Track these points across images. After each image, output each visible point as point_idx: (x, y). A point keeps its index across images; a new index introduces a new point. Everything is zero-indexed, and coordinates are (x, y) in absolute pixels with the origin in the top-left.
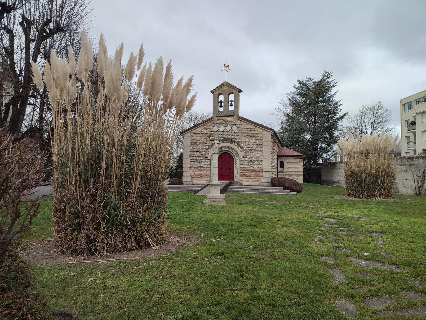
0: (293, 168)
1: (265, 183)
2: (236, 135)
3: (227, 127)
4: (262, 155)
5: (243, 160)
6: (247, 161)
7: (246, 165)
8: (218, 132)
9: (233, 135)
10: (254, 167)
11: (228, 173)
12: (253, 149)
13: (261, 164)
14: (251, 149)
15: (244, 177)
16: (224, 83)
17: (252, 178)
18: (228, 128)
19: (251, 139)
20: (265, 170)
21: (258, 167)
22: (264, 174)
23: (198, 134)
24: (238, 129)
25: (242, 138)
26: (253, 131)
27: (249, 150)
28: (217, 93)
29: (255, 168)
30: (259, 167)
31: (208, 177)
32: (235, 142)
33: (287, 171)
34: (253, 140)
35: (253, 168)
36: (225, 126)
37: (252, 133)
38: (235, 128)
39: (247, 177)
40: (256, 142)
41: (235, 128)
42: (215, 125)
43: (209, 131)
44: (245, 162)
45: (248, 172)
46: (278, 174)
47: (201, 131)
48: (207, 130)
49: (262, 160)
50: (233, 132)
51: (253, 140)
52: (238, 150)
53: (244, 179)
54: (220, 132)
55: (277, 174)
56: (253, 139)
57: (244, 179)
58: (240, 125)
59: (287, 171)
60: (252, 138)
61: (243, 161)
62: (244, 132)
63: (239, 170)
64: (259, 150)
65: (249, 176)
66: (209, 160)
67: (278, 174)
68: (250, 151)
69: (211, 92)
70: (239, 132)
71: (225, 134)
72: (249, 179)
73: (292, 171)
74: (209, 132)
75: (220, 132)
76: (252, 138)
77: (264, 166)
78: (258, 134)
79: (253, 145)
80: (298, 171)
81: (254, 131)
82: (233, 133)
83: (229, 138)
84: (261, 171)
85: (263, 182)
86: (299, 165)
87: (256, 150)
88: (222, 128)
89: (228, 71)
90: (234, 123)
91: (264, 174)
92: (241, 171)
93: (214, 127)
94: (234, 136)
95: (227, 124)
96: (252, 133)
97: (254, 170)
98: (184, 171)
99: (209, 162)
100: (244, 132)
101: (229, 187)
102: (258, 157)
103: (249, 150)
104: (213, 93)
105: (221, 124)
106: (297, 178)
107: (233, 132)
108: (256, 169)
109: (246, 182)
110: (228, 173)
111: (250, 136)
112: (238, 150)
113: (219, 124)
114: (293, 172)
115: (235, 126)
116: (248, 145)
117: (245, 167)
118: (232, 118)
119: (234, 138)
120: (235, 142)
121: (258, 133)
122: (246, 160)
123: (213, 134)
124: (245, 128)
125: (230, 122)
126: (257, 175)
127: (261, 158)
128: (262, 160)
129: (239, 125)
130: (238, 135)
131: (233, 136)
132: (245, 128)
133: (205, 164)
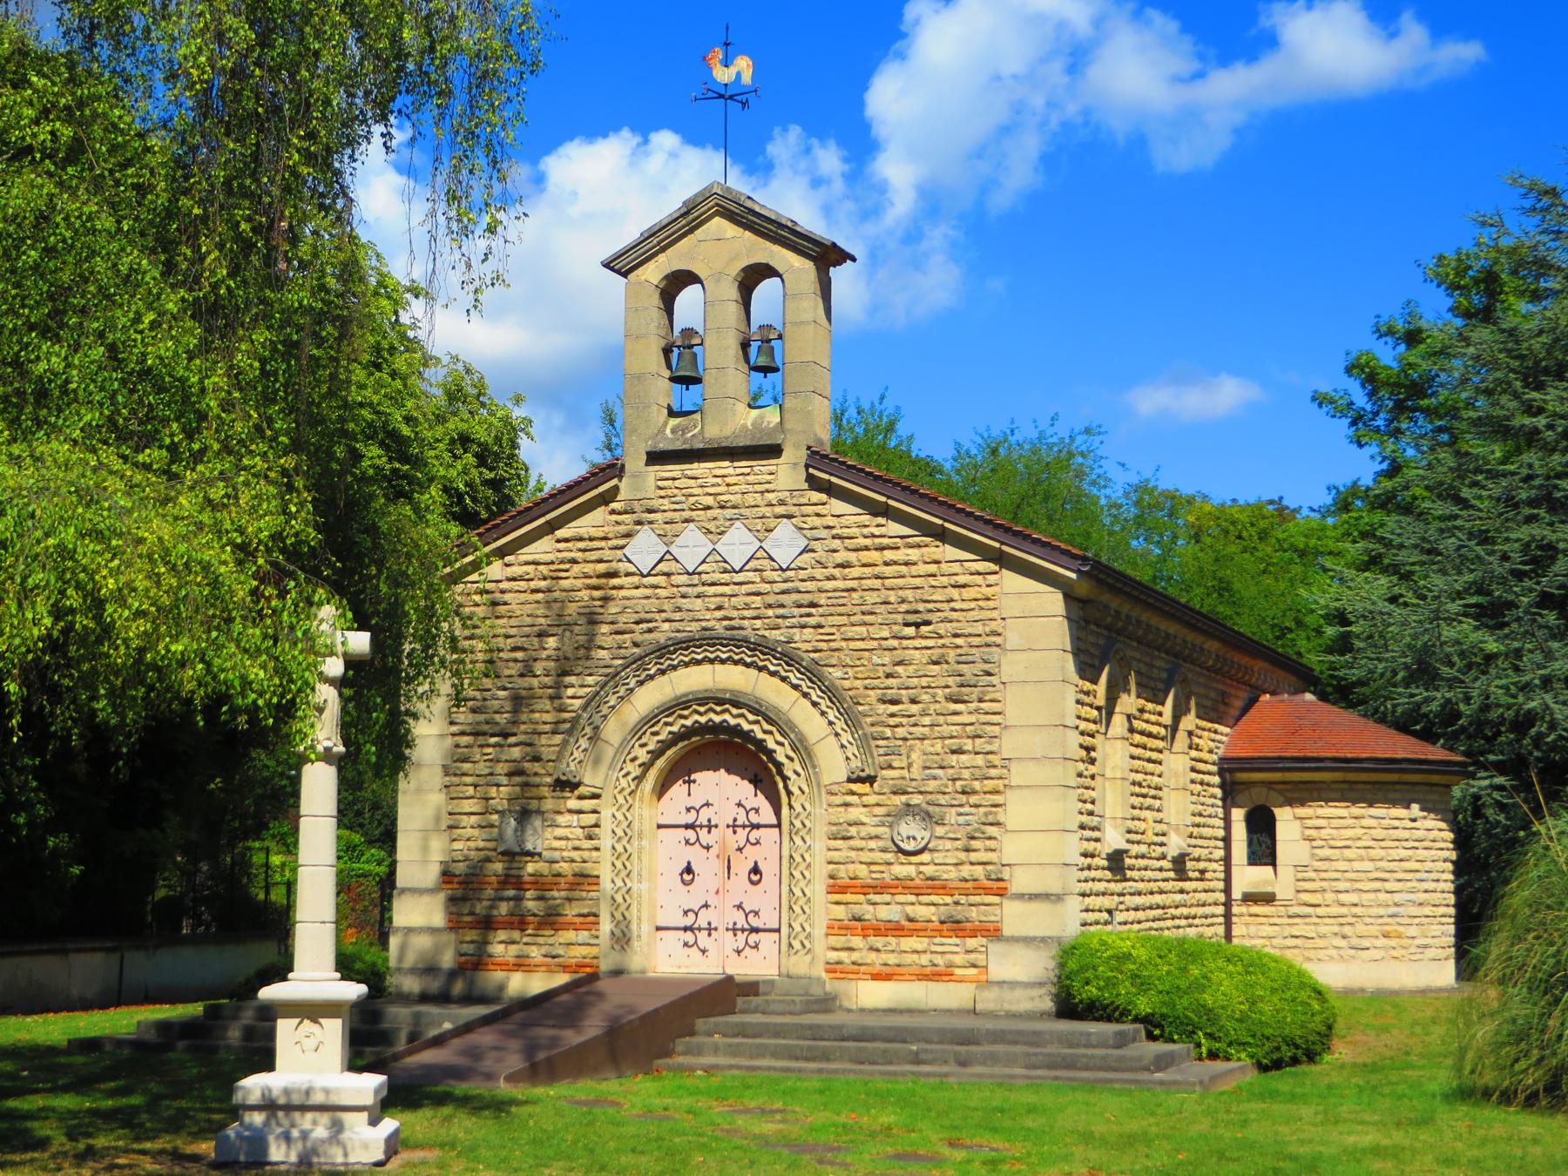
0: (1357, 865)
1: (1019, 993)
2: (795, 597)
3: (725, 538)
4: (995, 759)
5: (846, 805)
6: (878, 811)
7: (872, 844)
8: (661, 580)
9: (771, 599)
10: (938, 857)
11: (740, 907)
12: (924, 714)
13: (992, 831)
14: (915, 708)
15: (857, 941)
16: (705, 196)
17: (919, 947)
18: (737, 545)
19: (911, 631)
20: (1021, 881)
21: (963, 855)
22: (1015, 917)
23: (507, 597)
24: (805, 550)
25: (844, 620)
26: (922, 569)
27: (892, 721)
28: (654, 273)
29: (945, 862)
30: (974, 856)
31: (583, 936)
32: (790, 659)
33: (1307, 885)
34: (930, 643)
35: (929, 870)
36: (711, 526)
37: (918, 582)
38: (785, 544)
39: (878, 942)
40: (952, 655)
41: (785, 544)
42: (639, 523)
43: (589, 568)
44: (864, 813)
45: (887, 898)
46: (1235, 910)
47: (530, 568)
48: (574, 561)
49: (998, 799)
50: (776, 576)
51: (930, 643)
52: (809, 720)
53: (855, 956)
54: (677, 579)
55: (1220, 910)
56: (924, 629)
57: (855, 956)
58: (830, 521)
59: (1307, 885)
60: (917, 625)
61: (855, 813)
62: (856, 572)
63: (818, 889)
64: (972, 719)
65: (895, 929)
66: (588, 804)
67: (1228, 916)
68: (901, 732)
69: (607, 265)
70: (819, 573)
71: (712, 590)
72: (892, 959)
73: (1341, 886)
74: (594, 581)
75: (677, 579)
76: (917, 625)
77: (1012, 848)
78: (968, 593)
79: (924, 681)
80: (1398, 886)
81: (933, 568)
82: (778, 587)
83: (746, 623)
84: (988, 891)
85: (1000, 983)
86: (1406, 834)
87: (952, 719)
88: (691, 547)
89: (744, 104)
90: (782, 503)
91: (1015, 917)
92: (836, 887)
93: (628, 535)
94: (782, 606)
95: (729, 513)
96: (918, 582)
97: (934, 885)
98: (403, 891)
99: (589, 819)
100: (856, 572)
101: (700, 1024)
102: (966, 774)
103: (892, 721)
104: (625, 275)
105: (687, 514)
106: (1393, 942)
107: (776, 576)
108: (951, 874)
109: (876, 977)
110: (740, 907)
111: (904, 607)
112: (809, 720)
113: (669, 515)
114: (1353, 898)
115: (785, 529)
116: (890, 682)
117: (866, 856)
118: (762, 467)
119: (777, 628)
120: (790, 659)
121: (962, 579)
122: (872, 799)
123: (623, 593)
124: (868, 542)
125: (750, 500)
126: (955, 926)
127: (989, 784)
128: (998, 799)
129: (817, 521)
130: (806, 598)
131: (770, 606)
132: (868, 542)
133: (559, 832)
